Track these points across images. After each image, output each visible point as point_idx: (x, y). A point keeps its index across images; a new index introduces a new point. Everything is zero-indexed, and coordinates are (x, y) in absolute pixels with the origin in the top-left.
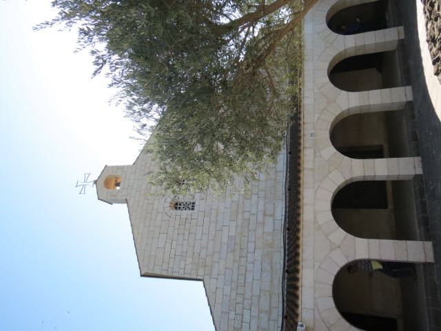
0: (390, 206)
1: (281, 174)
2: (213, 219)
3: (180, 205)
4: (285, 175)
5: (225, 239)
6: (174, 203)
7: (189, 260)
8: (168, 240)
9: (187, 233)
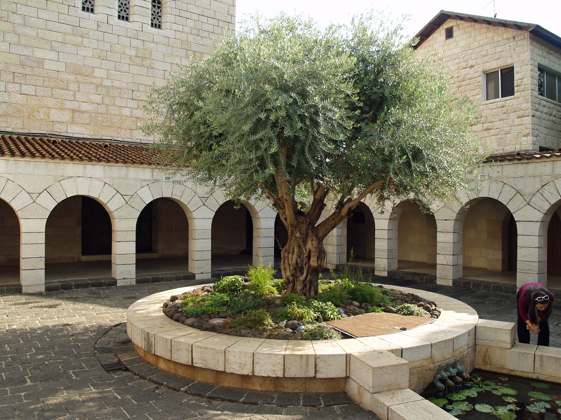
0: (85, 258)
1: (128, 135)
2: (69, 38)
4: (125, 140)
5: (39, 54)
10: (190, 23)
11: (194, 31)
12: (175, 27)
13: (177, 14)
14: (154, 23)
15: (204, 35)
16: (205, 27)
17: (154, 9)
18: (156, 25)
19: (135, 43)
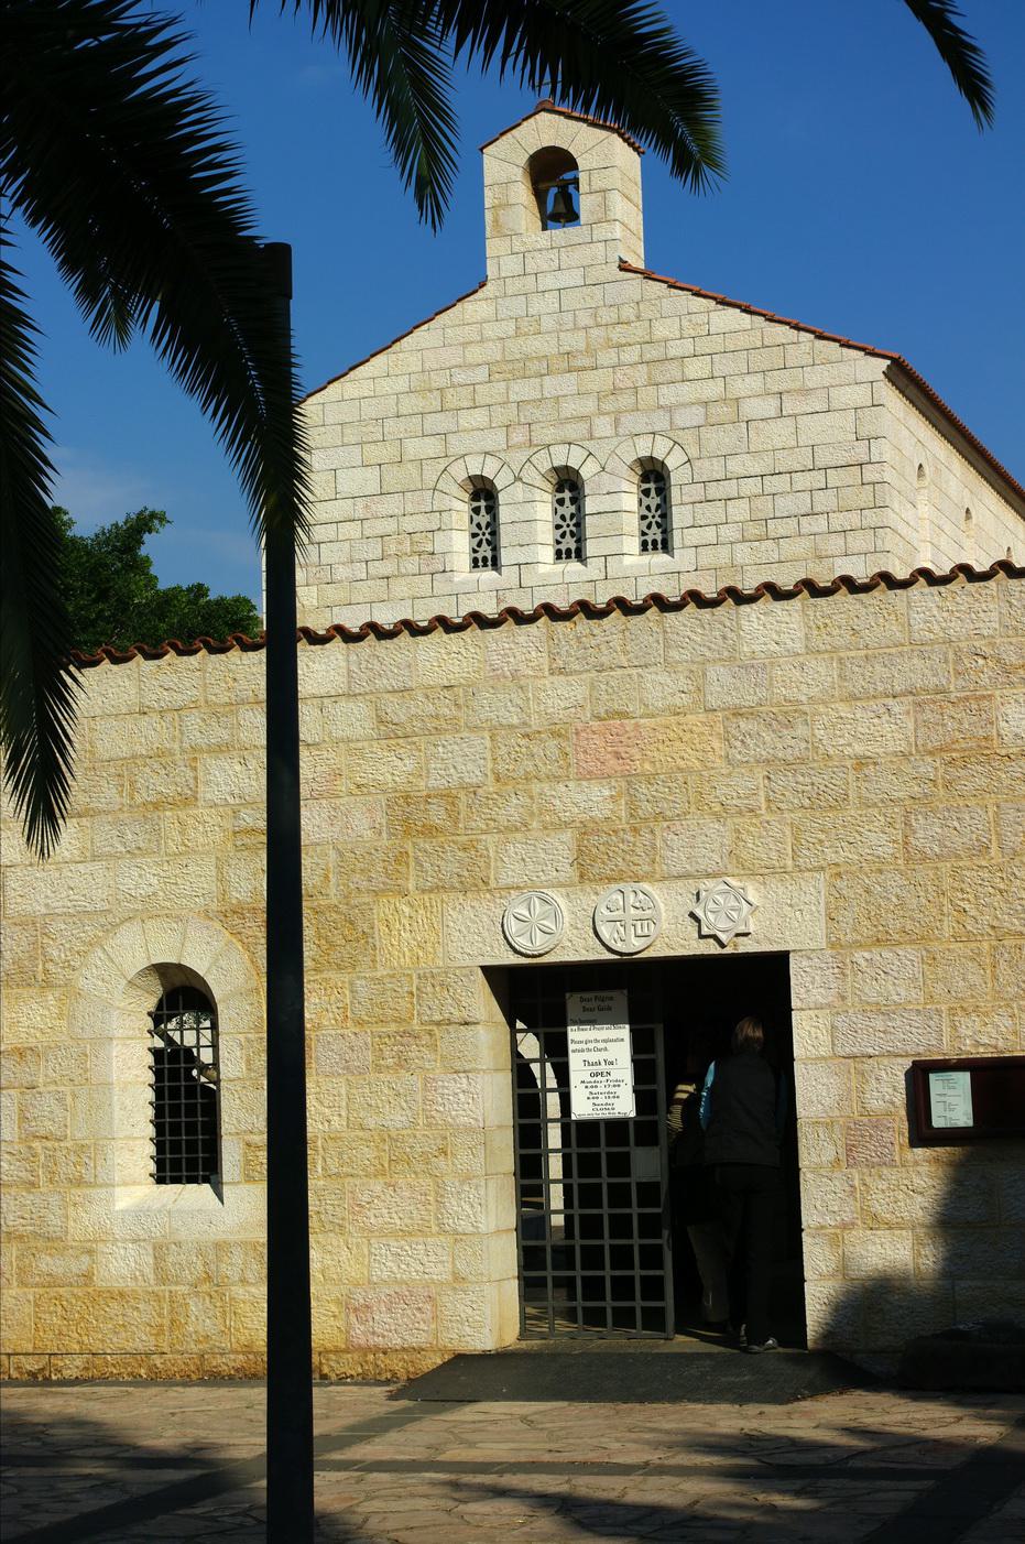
10: (739, 510)
11: (754, 530)
12: (694, 536)
13: (698, 499)
14: (649, 539)
15: (781, 532)
16: (785, 505)
17: (645, 501)
18: (655, 542)
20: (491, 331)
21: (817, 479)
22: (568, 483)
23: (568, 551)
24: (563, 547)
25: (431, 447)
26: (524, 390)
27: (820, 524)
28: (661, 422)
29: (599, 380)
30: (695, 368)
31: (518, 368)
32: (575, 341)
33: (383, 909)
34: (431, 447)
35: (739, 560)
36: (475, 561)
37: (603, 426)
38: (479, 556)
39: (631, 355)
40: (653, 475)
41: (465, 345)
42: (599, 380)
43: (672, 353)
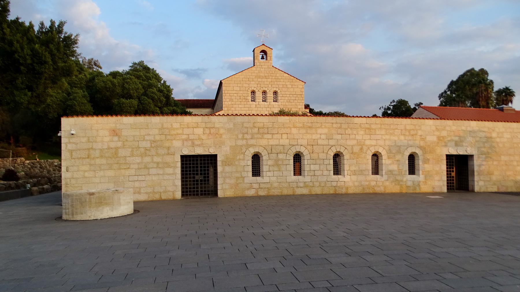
3: (253, 94)
6: (254, 91)
7: (230, 103)
8: (237, 91)
9: (241, 100)
10: (286, 98)
11: (288, 101)
12: (281, 101)
14: (274, 100)
16: (293, 98)
19: (268, 109)
20: (256, 72)
21: (296, 96)
22: (264, 92)
23: (264, 101)
24: (263, 100)
25: (247, 85)
26: (259, 80)
27: (296, 101)
28: (277, 86)
29: (269, 80)
30: (282, 80)
31: (260, 77)
32: (267, 75)
33: (437, 147)
34: (247, 85)
35: (287, 104)
36: (251, 101)
37: (270, 86)
38: (263, 100)
39: (274, 78)
40: (275, 93)
41: (252, 73)
42: (269, 80)
43: (279, 78)
